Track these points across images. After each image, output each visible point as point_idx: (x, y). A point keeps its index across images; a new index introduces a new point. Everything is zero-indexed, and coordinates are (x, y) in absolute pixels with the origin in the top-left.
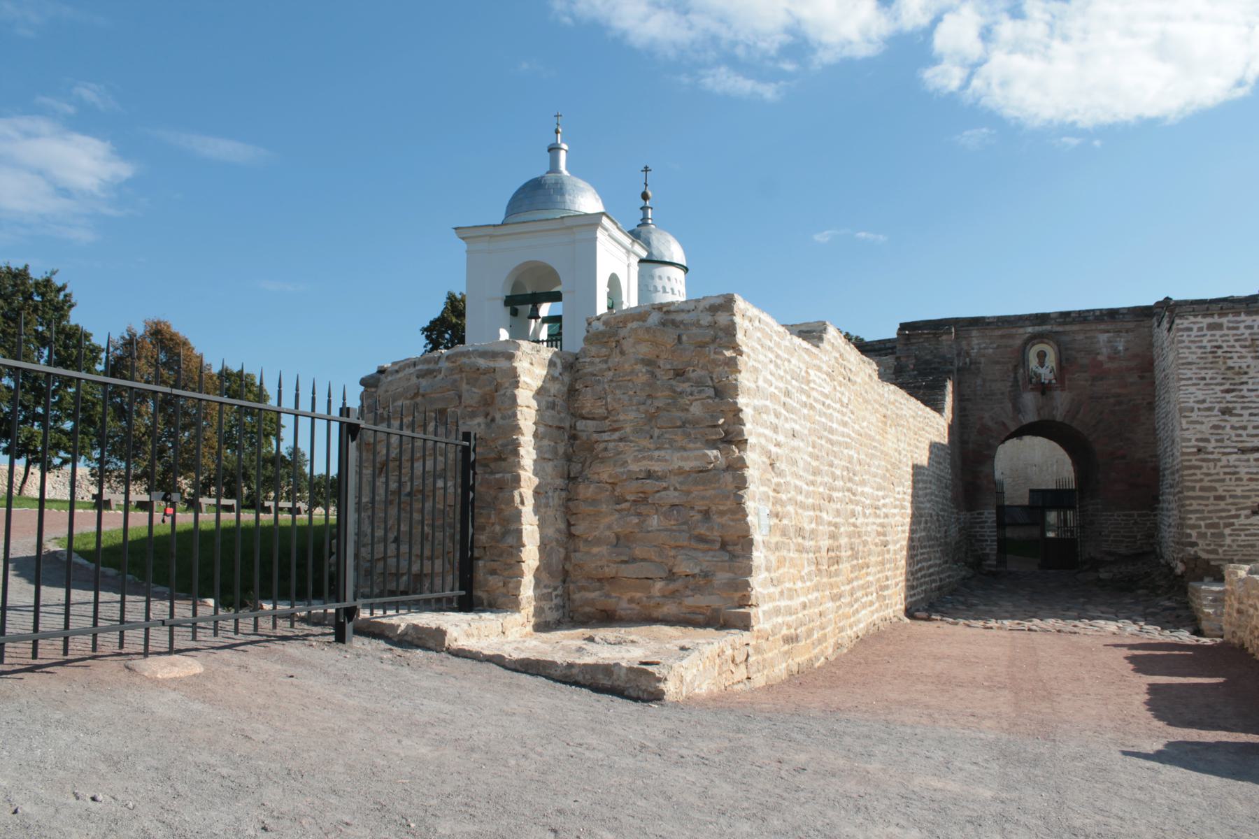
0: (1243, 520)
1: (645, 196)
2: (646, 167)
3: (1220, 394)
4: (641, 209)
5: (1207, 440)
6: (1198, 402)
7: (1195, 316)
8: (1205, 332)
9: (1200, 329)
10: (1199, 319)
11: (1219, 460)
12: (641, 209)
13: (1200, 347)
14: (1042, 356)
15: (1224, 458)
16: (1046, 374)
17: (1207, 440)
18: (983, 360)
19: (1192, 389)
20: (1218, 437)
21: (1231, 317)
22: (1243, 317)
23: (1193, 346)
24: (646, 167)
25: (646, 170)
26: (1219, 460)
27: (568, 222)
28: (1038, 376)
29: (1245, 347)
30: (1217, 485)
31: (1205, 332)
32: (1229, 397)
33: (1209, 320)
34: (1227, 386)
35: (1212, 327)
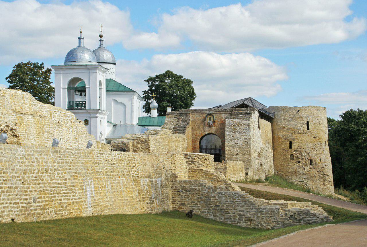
0: (235, 156)
1: (101, 36)
2: (101, 25)
3: (232, 133)
4: (100, 41)
5: (229, 142)
6: (228, 135)
7: (229, 118)
8: (230, 122)
9: (229, 121)
10: (229, 119)
11: (231, 145)
12: (100, 41)
13: (229, 125)
14: (210, 118)
15: (232, 145)
16: (211, 123)
17: (229, 142)
18: (197, 119)
19: (227, 132)
20: (231, 141)
21: (235, 119)
22: (237, 119)
23: (228, 124)
24: (101, 25)
25: (101, 26)
26: (231, 145)
27: (88, 67)
28: (209, 123)
29: (236, 125)
30: (231, 150)
31: (230, 122)
32: (233, 134)
33: (232, 119)
34: (233, 132)
35: (231, 121)
